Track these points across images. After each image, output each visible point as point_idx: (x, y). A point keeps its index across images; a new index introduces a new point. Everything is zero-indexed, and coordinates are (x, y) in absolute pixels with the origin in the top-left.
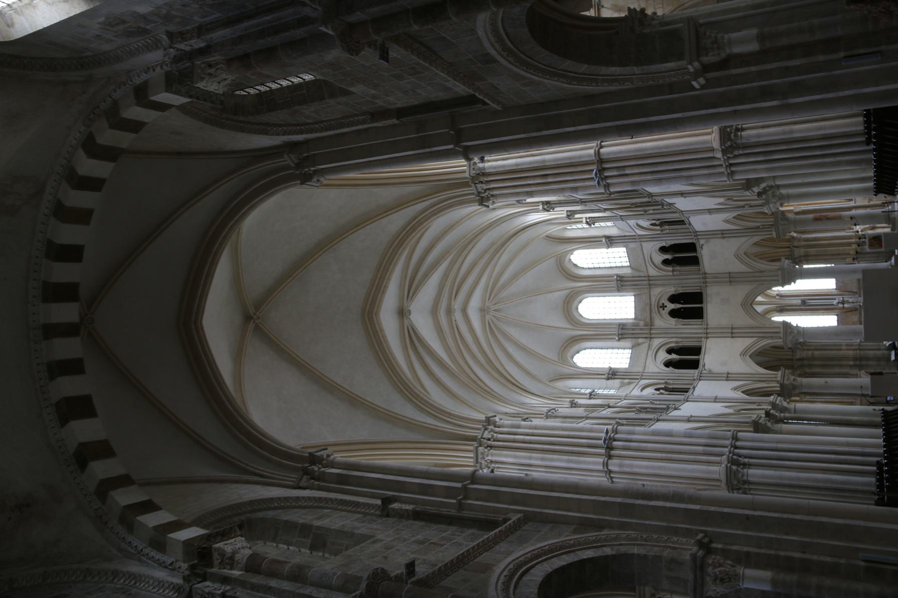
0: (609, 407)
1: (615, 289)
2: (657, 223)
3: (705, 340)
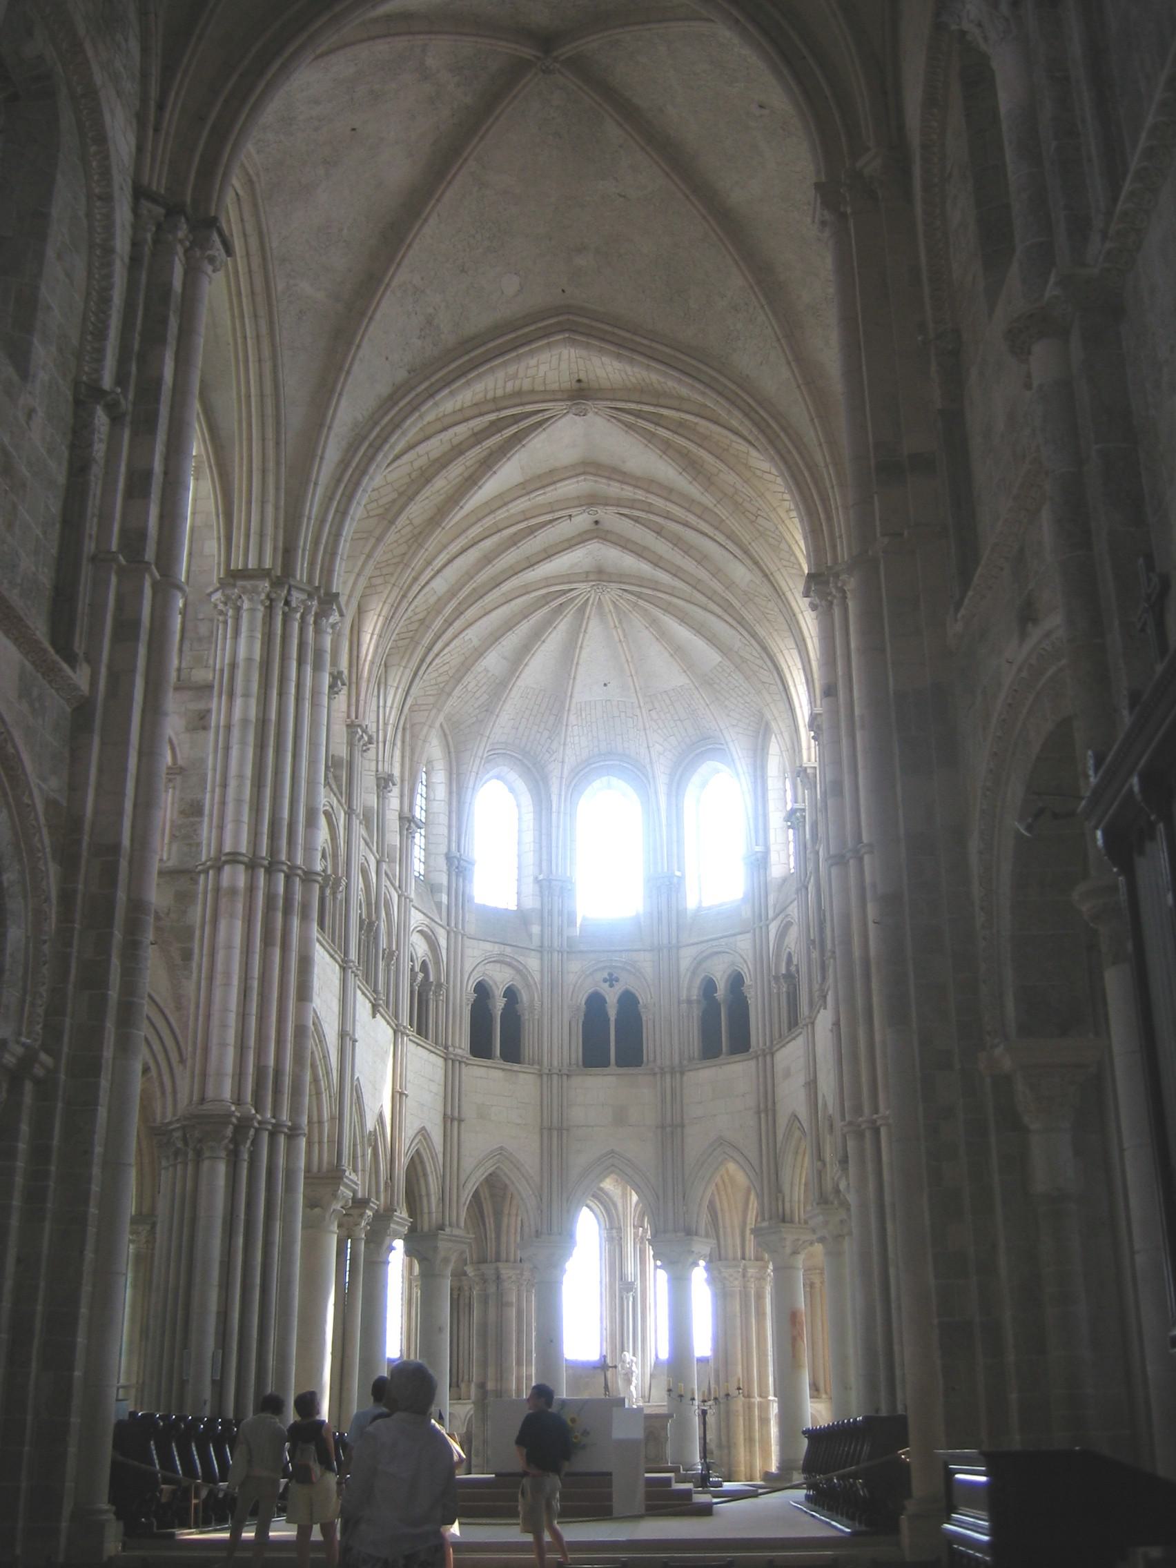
2: (793, 969)
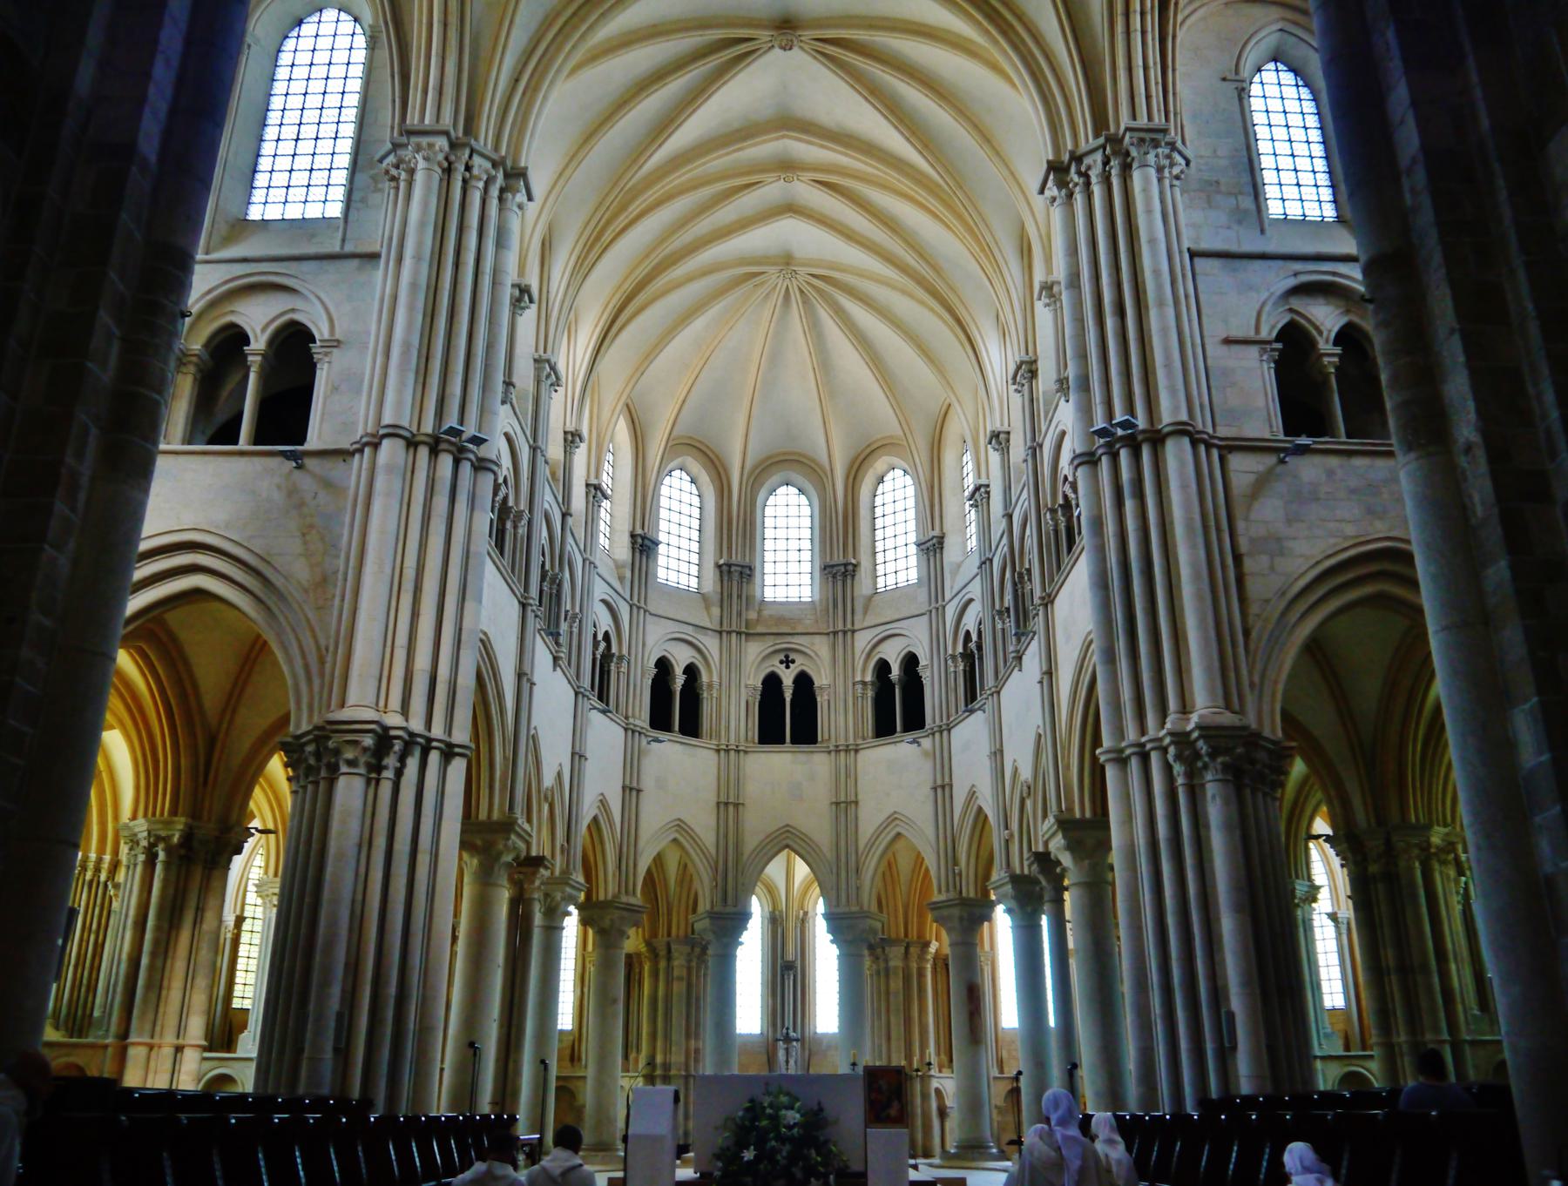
0: (565, 515)
1: (828, 560)
2: (972, 645)
3: (715, 747)
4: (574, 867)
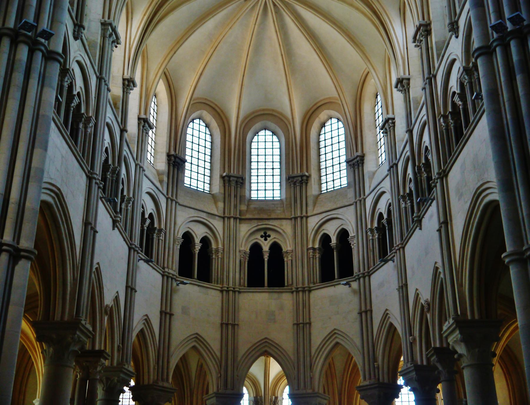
2: (384, 221)
3: (219, 289)
4: (127, 362)
